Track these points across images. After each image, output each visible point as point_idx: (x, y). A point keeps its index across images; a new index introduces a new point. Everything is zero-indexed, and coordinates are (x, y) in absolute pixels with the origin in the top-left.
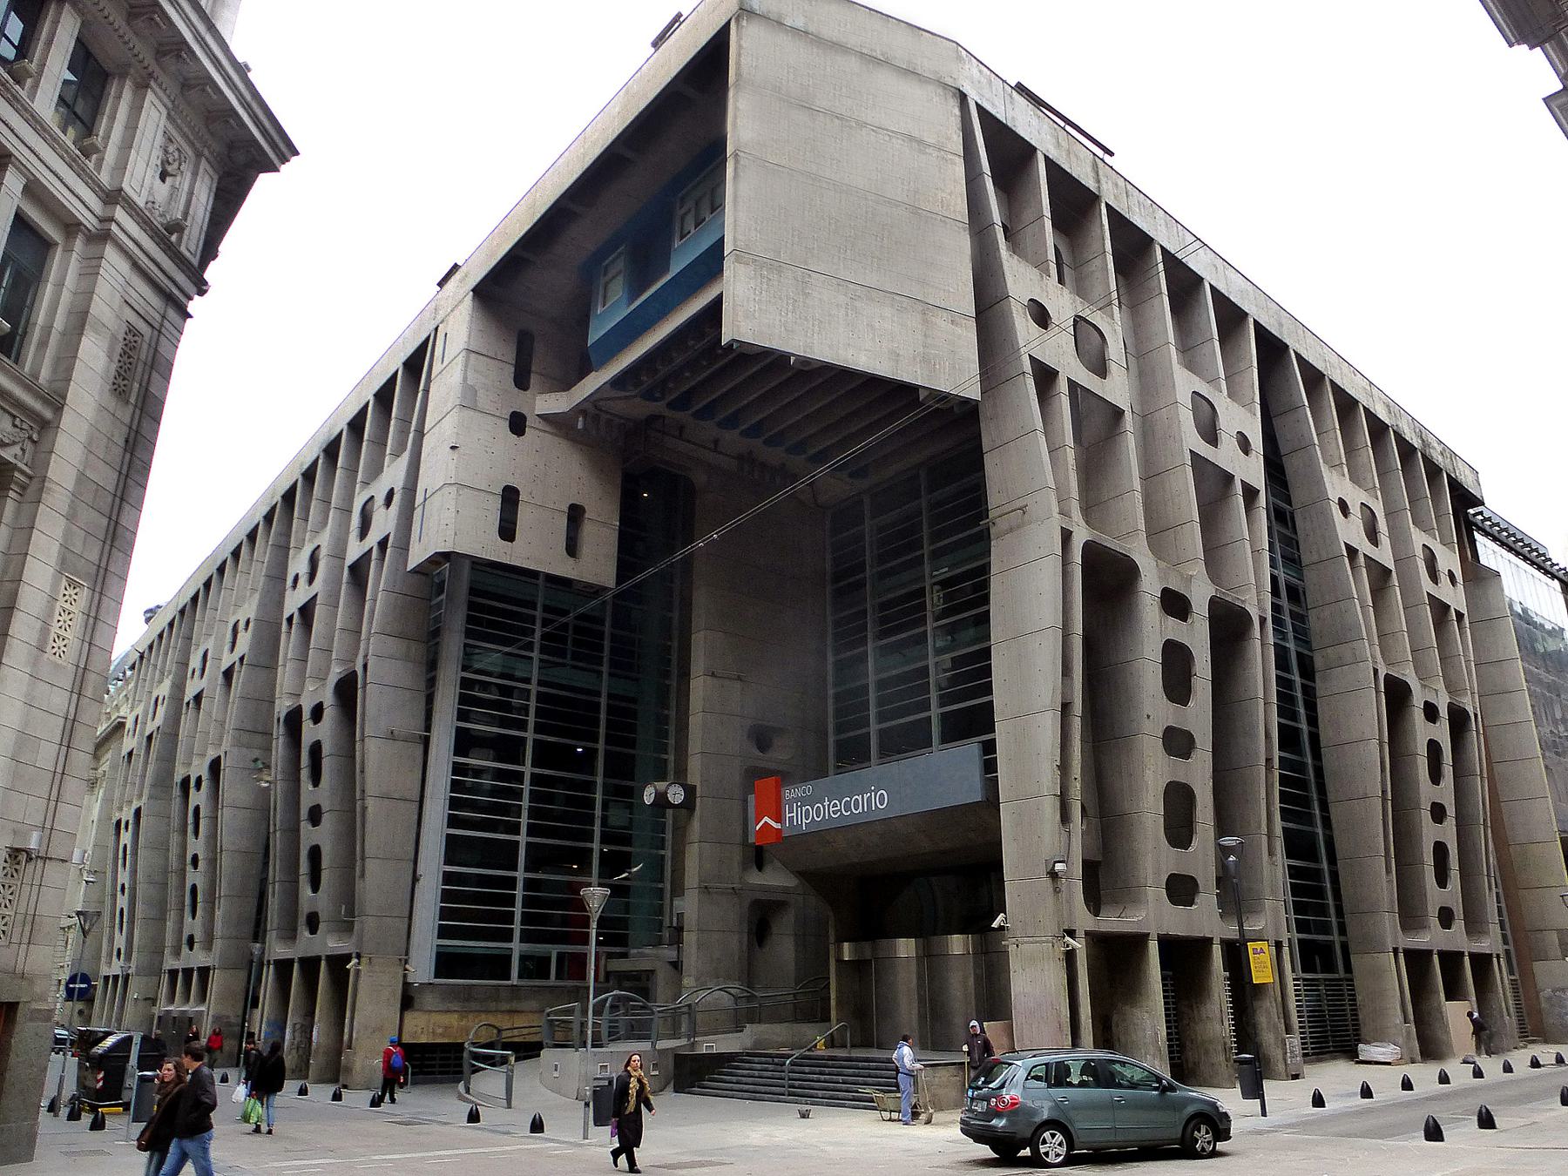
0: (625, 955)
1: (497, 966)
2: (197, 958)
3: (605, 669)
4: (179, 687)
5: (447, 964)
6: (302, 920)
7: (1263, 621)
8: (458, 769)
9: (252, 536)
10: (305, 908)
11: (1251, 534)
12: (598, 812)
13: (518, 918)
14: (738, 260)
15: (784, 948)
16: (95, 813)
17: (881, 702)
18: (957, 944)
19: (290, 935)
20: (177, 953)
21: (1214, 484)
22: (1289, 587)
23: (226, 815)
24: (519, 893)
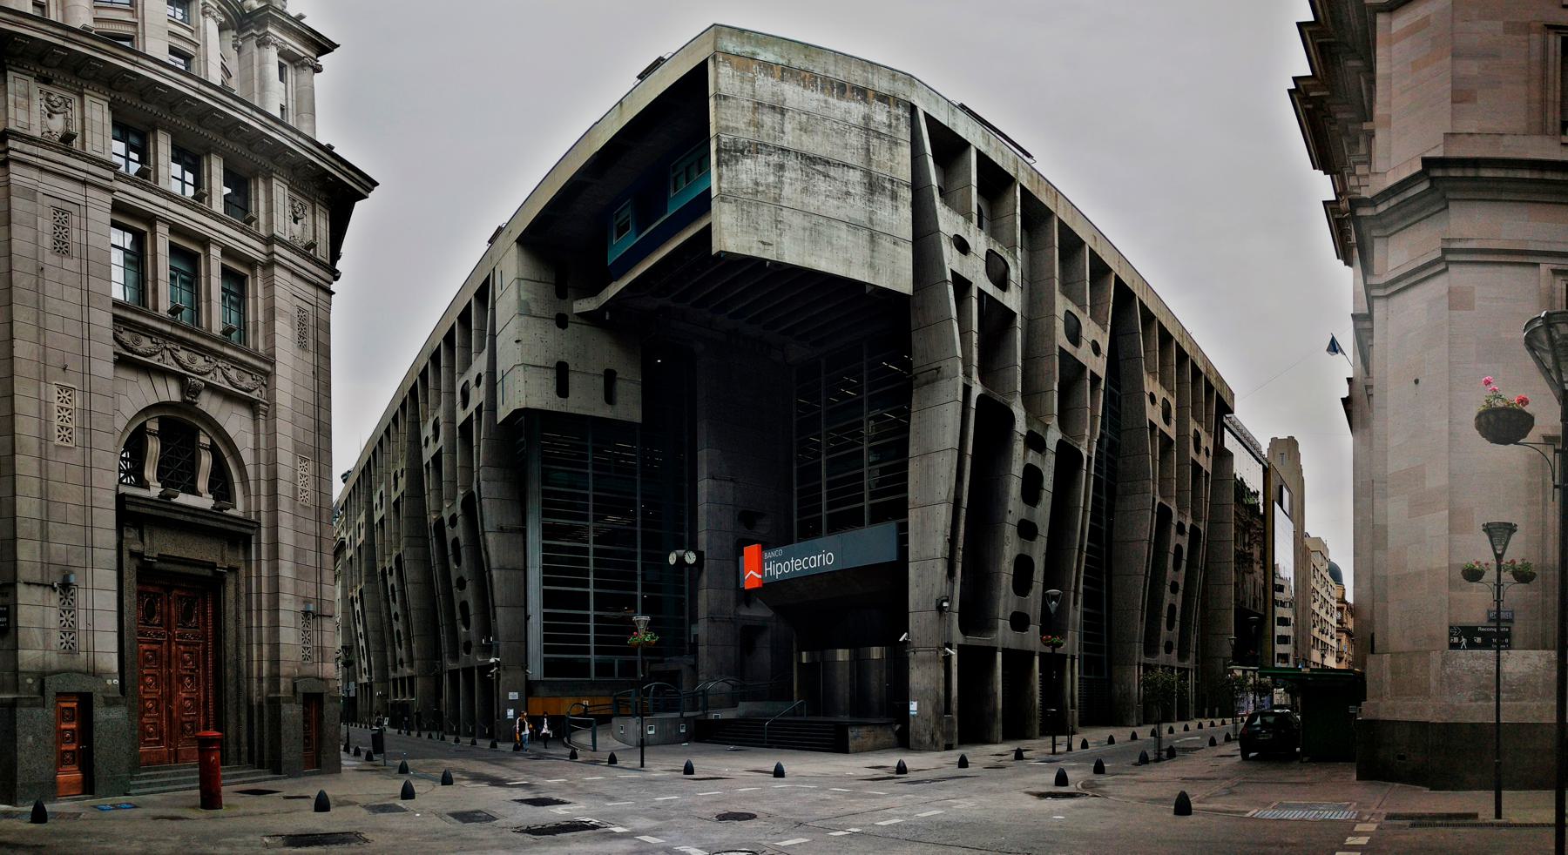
0: (662, 661)
1: (583, 669)
2: (407, 671)
3: (638, 477)
4: (370, 516)
5: (549, 667)
6: (461, 646)
7: (1089, 459)
8: (545, 548)
9: (395, 419)
10: (462, 639)
11: (1092, 406)
12: (639, 571)
13: (592, 639)
14: (723, 200)
15: (764, 656)
16: (339, 595)
17: (829, 495)
18: (876, 652)
19: (455, 657)
20: (395, 670)
21: (1073, 371)
22: (1111, 442)
23: (409, 588)
24: (592, 624)
